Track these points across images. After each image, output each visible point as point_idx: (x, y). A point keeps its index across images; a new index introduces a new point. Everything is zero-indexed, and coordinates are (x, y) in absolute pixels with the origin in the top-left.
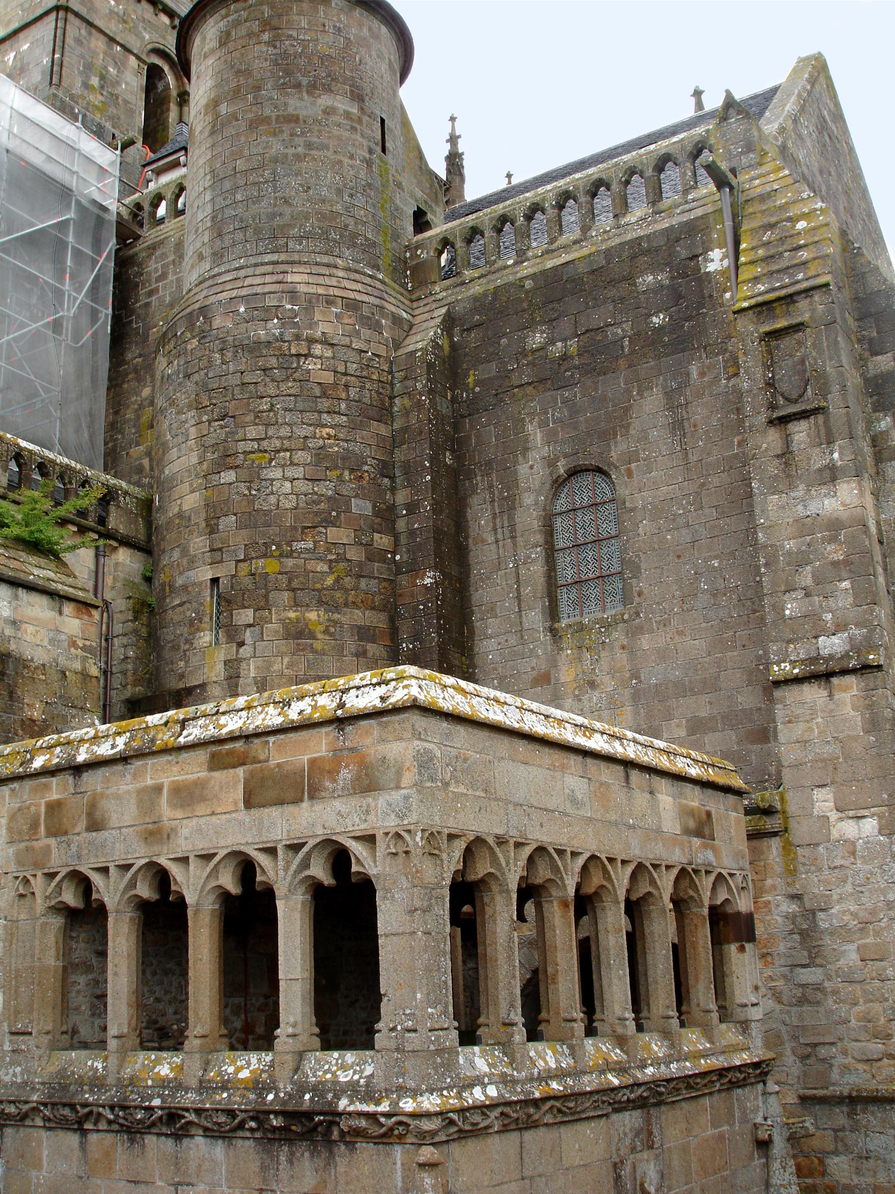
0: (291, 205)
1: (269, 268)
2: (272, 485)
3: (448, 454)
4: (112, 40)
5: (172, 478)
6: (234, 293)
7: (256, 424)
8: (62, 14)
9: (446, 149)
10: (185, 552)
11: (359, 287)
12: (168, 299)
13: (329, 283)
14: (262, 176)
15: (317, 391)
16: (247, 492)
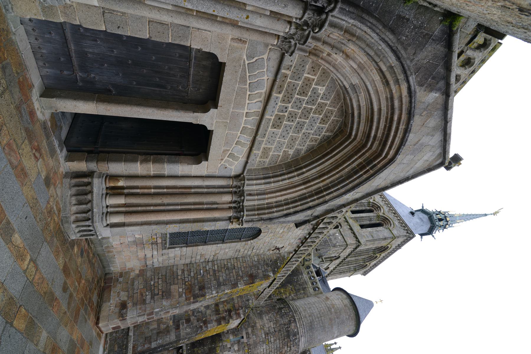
1: (304, 332)
4: (342, 252)
5: (263, 319)
6: (299, 327)
10: (248, 327)
12: (295, 287)
15: (281, 351)
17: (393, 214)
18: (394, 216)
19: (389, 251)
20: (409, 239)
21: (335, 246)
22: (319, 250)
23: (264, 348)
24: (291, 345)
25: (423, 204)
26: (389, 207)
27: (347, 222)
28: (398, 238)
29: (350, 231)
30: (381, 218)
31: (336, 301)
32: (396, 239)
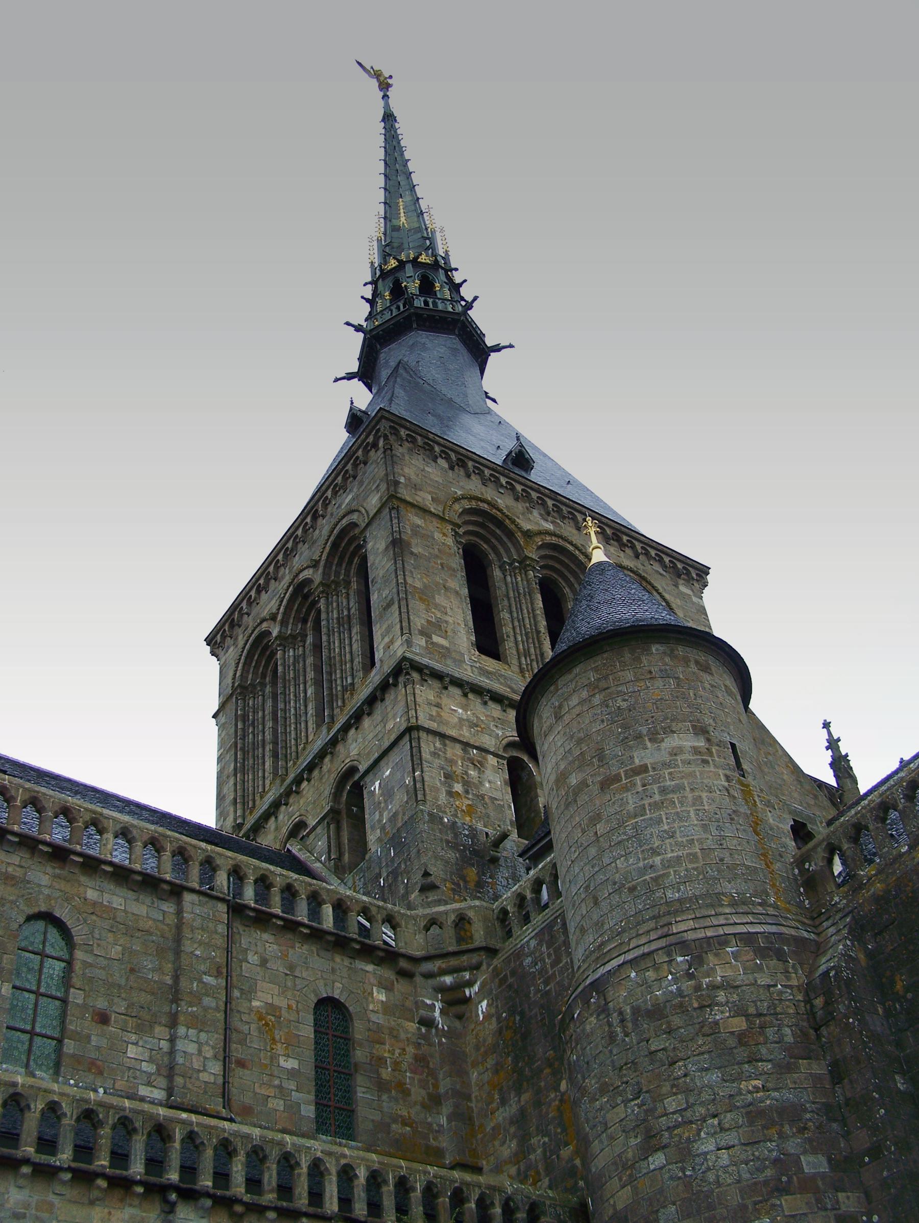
0: (659, 854)
1: (652, 924)
2: (706, 1160)
3: (897, 1077)
4: (466, 745)
6: (621, 960)
7: (675, 1094)
8: (415, 734)
9: (828, 756)
11: (750, 918)
13: (716, 923)
14: (624, 833)
15: (732, 1042)
16: (680, 1174)
17: (320, 521)
18: (323, 517)
19: (504, 501)
20: (403, 432)
21: (416, 792)
22: (426, 874)
23: (712, 1147)
24: (698, 988)
25: (336, 380)
26: (296, 543)
27: (334, 742)
28: (397, 483)
29: (366, 722)
30: (337, 574)
31: (549, 770)
32: (405, 493)
